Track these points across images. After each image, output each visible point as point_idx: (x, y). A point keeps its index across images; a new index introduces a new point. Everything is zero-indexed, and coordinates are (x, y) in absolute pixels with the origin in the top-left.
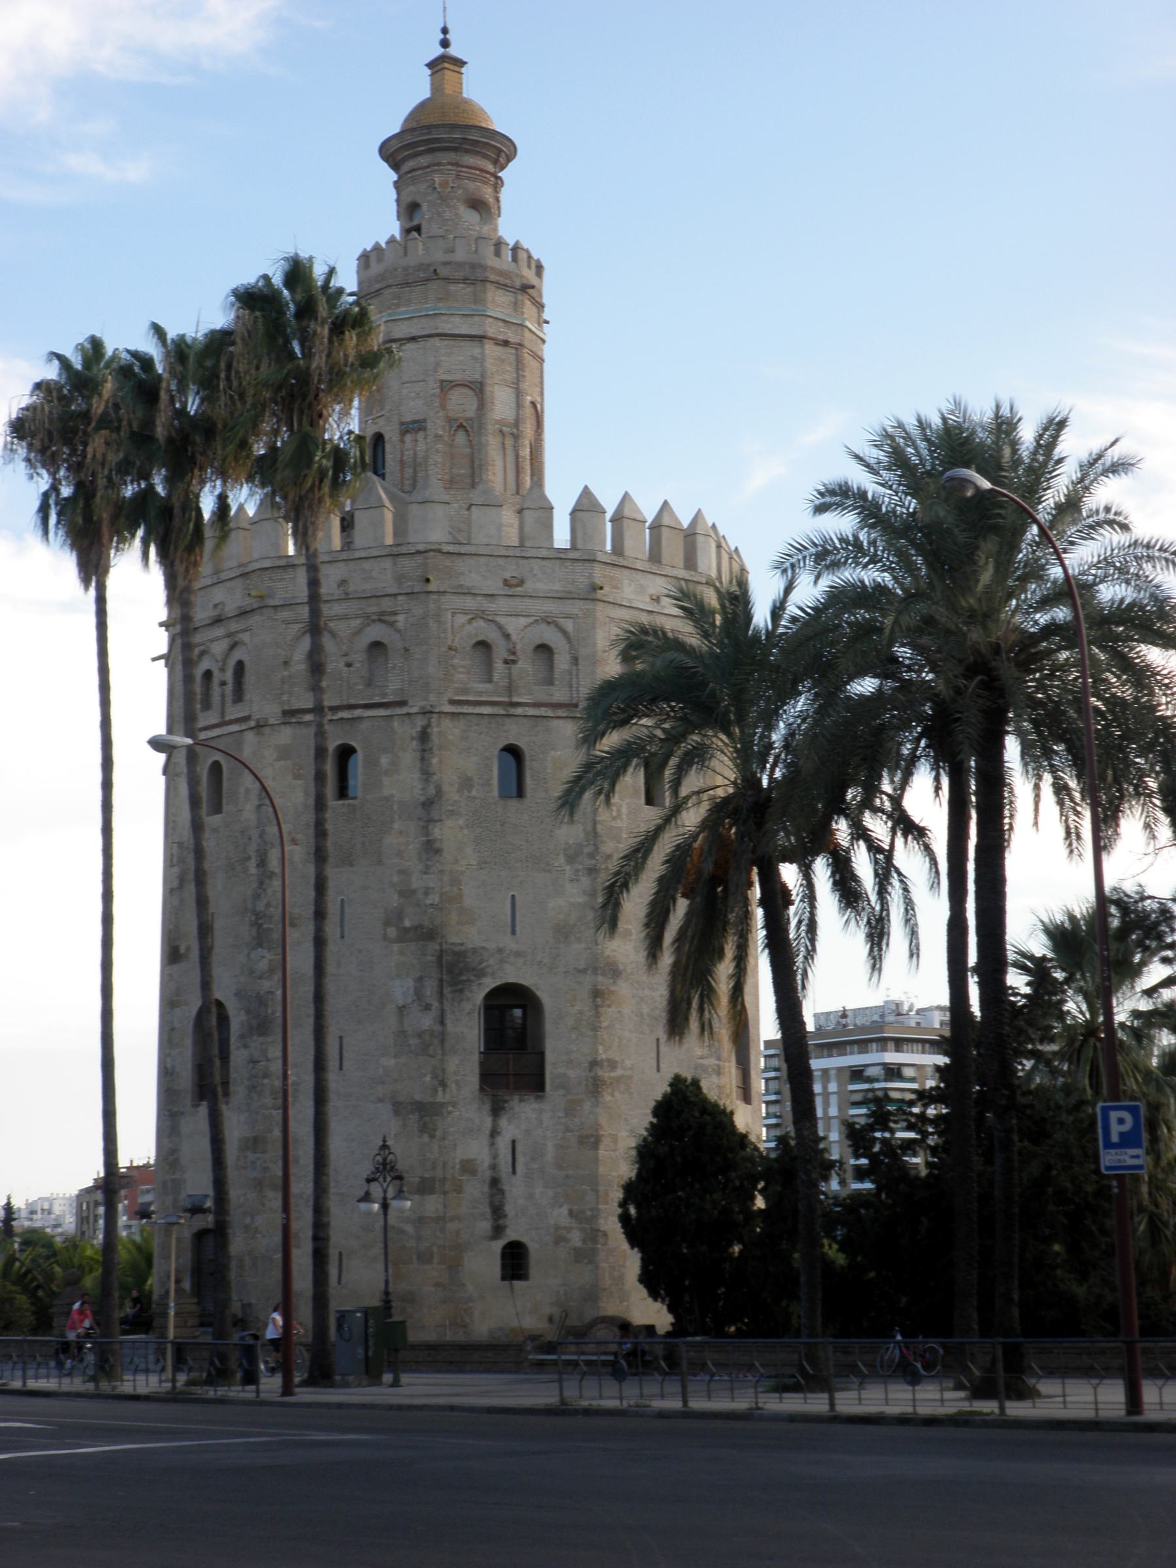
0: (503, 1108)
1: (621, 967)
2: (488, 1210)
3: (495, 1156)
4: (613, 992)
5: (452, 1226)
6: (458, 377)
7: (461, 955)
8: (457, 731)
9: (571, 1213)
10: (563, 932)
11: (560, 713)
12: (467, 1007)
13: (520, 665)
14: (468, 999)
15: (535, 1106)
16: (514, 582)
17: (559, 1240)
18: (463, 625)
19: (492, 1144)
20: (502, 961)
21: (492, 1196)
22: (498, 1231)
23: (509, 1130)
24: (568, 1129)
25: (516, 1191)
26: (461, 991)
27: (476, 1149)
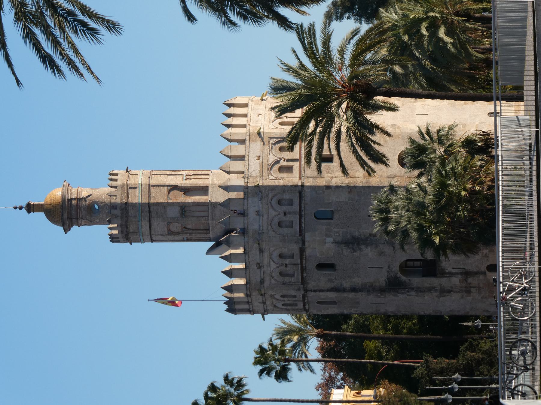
6: (166, 229)
8: (312, 283)
10: (381, 254)
13: (287, 263)
16: (258, 266)
18: (275, 280)
20: (391, 271)
23: (449, 269)
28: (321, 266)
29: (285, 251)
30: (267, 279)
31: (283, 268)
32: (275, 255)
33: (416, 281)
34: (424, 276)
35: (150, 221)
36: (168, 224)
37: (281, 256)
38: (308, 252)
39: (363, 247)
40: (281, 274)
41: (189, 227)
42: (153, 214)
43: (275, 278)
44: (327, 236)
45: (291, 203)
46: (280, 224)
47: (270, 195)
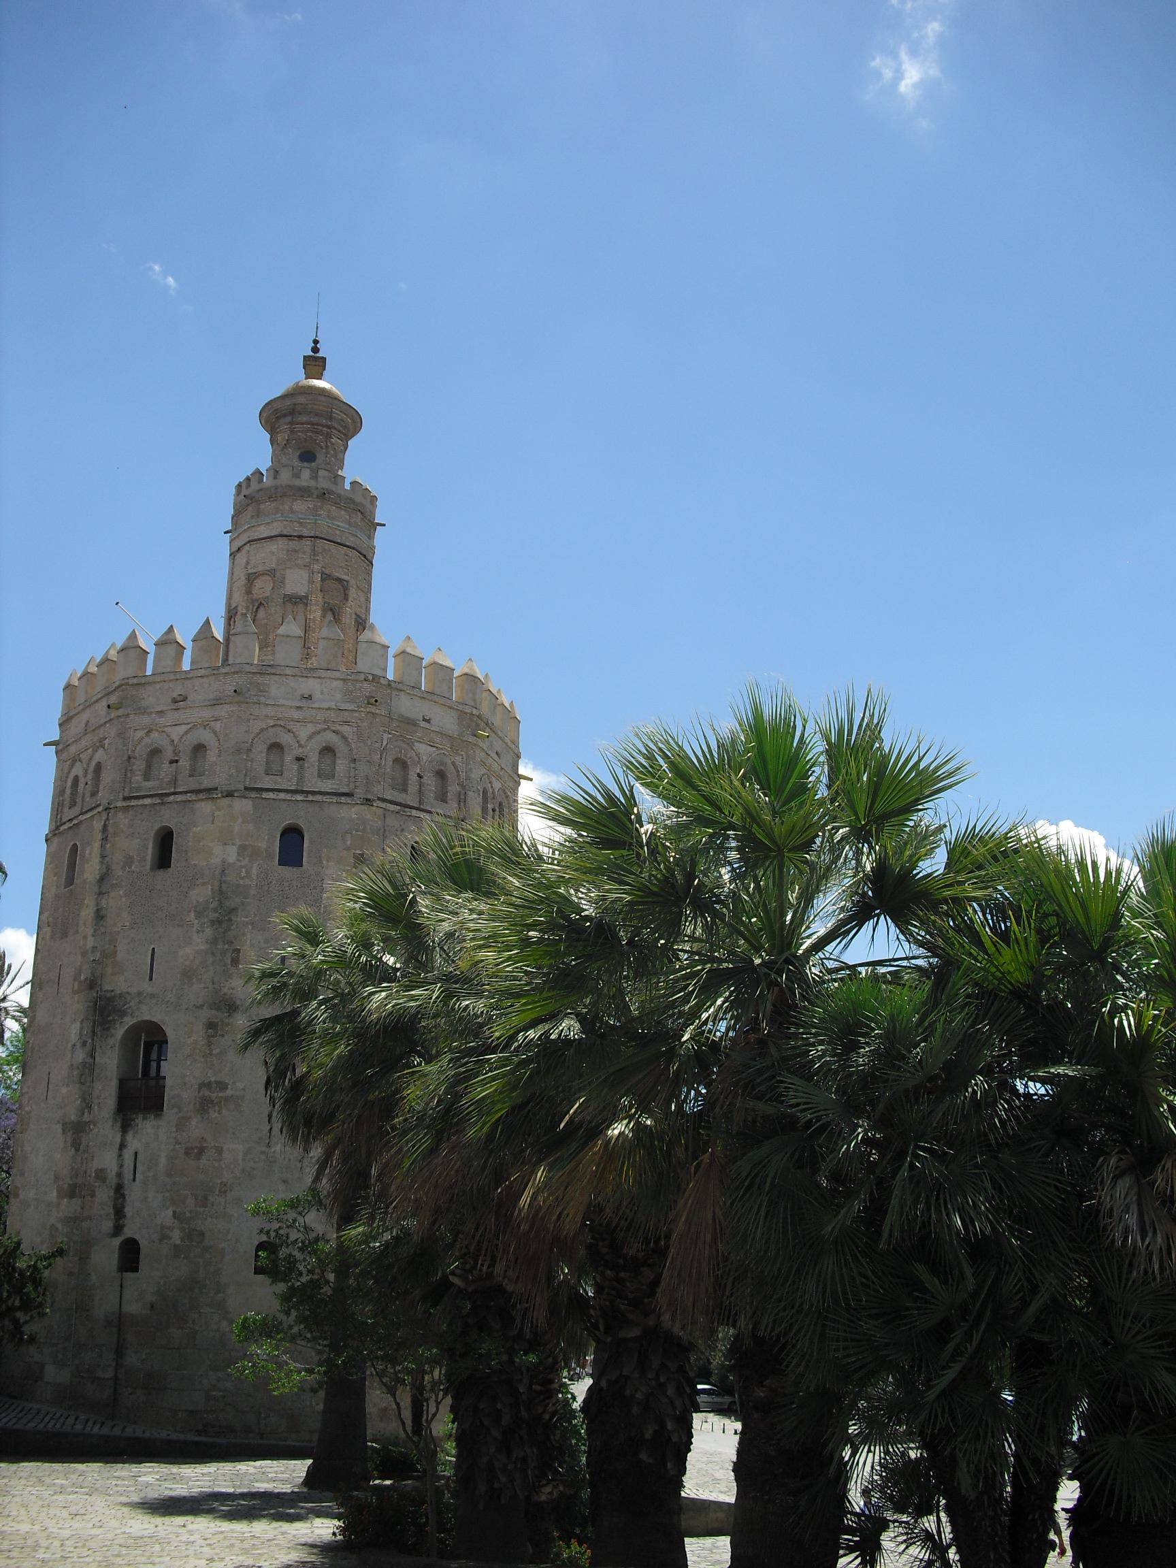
0: (129, 1125)
1: (238, 1002)
2: (112, 1211)
3: (121, 1166)
4: (228, 1024)
5: (85, 1225)
6: (260, 568)
7: (111, 1000)
9: (174, 1212)
10: (188, 975)
11: (201, 796)
12: (111, 1041)
13: (181, 763)
14: (112, 1035)
15: (155, 1122)
17: (164, 1237)
18: (142, 739)
20: (140, 1002)
21: (116, 1199)
23: (134, 1143)
24: (177, 1142)
25: (134, 1194)
26: (108, 1029)
28: (165, 841)
29: (212, 756)
30: (146, 720)
31: (169, 754)
32: (206, 736)
33: (110, 1062)
34: (122, 1083)
35: (282, 536)
36: (272, 573)
37: (200, 748)
38: (205, 807)
39: (209, 932)
40: (155, 752)
42: (294, 544)
43: (147, 740)
44: (242, 849)
45: (321, 775)
46: (276, 747)
47: (346, 729)
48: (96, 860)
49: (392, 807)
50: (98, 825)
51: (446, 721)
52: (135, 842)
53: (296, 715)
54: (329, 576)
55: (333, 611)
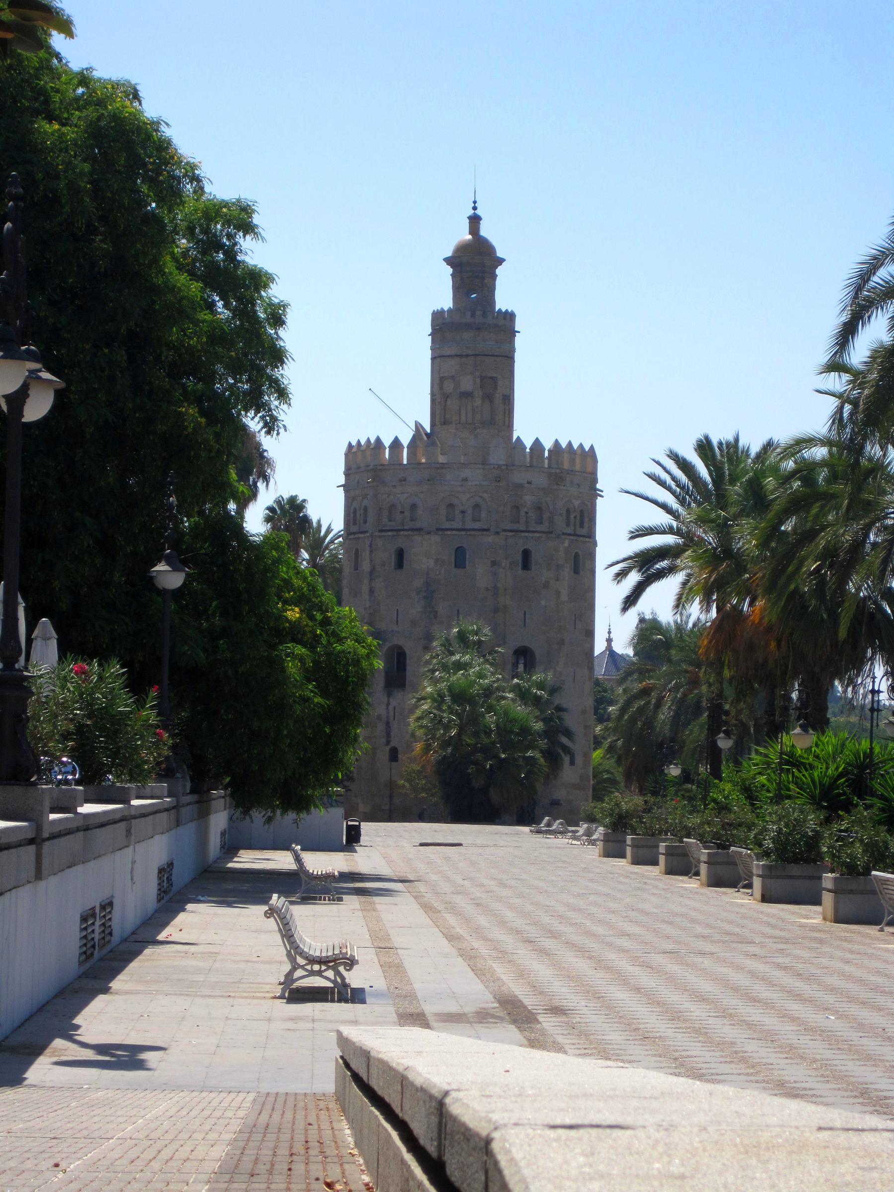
3: (388, 713)
19: (387, 708)
22: (388, 742)
23: (394, 703)
27: (381, 710)
28: (400, 555)
35: (457, 356)
36: (453, 377)
37: (413, 507)
40: (392, 506)
41: (449, 402)
44: (436, 561)
45: (474, 520)
46: (451, 506)
47: (485, 495)
48: (368, 561)
49: (510, 534)
50: (368, 542)
51: (540, 480)
52: (386, 555)
53: (460, 489)
54: (485, 377)
55: (489, 397)
